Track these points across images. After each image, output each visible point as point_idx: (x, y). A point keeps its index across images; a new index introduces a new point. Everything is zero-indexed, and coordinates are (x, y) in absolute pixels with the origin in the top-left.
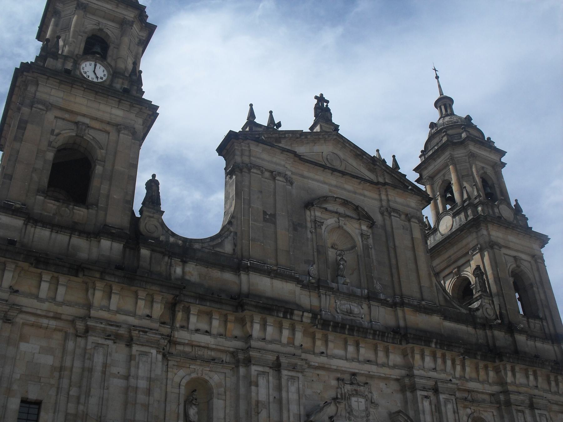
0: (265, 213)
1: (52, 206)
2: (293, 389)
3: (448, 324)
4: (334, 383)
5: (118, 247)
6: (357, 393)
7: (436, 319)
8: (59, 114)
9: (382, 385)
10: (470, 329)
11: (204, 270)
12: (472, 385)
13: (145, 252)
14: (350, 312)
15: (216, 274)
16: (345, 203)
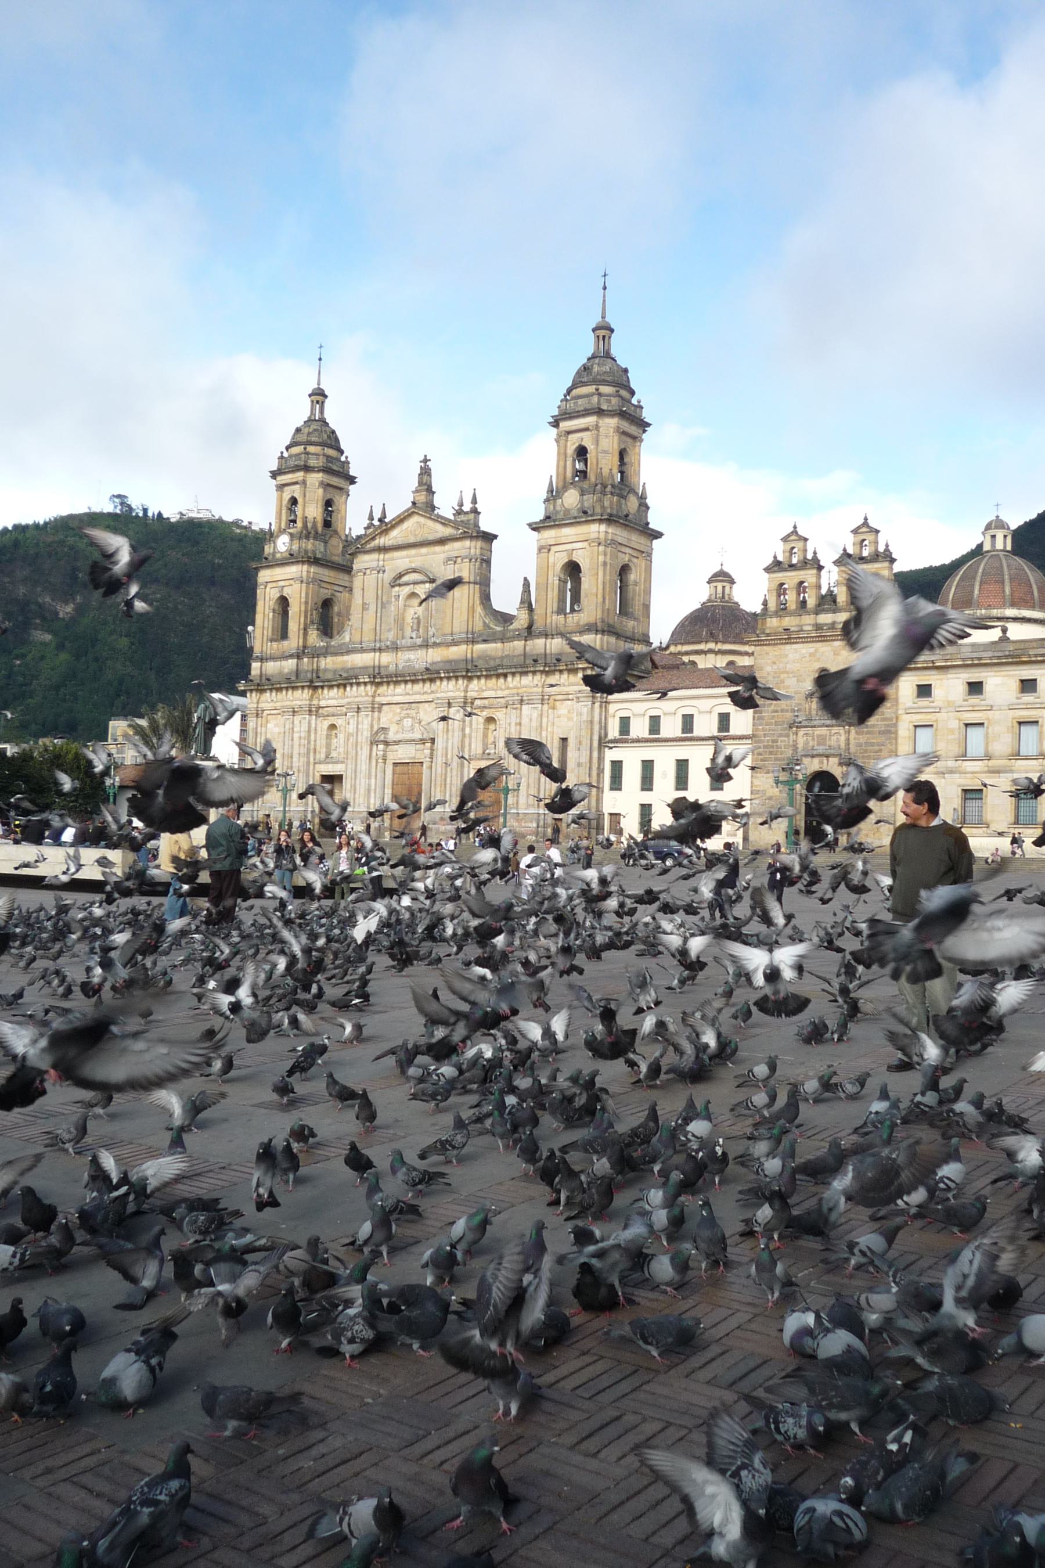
0: (364, 604)
1: (275, 644)
2: (366, 722)
3: (480, 647)
4: (398, 711)
5: (295, 661)
6: (408, 716)
7: (464, 647)
8: (270, 585)
9: (426, 705)
10: (499, 645)
11: (334, 658)
12: (486, 694)
13: (306, 660)
14: (409, 660)
15: (340, 659)
16: (414, 571)
